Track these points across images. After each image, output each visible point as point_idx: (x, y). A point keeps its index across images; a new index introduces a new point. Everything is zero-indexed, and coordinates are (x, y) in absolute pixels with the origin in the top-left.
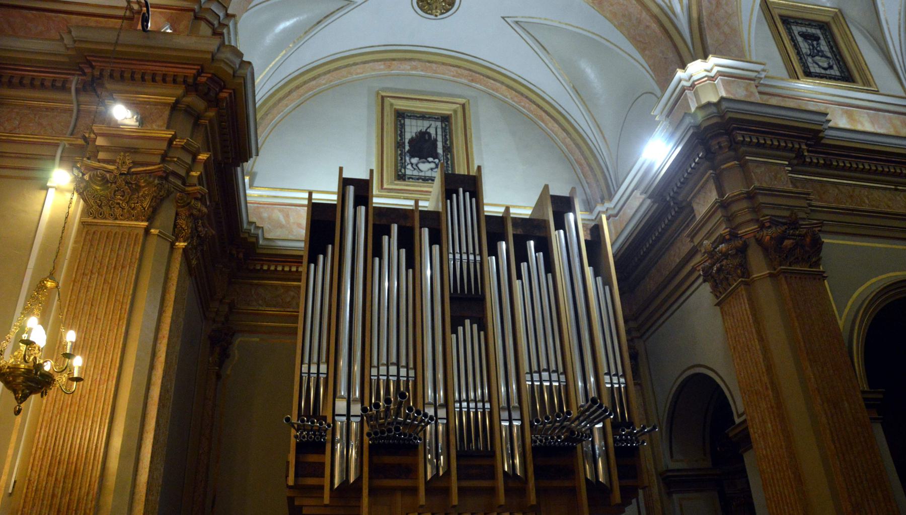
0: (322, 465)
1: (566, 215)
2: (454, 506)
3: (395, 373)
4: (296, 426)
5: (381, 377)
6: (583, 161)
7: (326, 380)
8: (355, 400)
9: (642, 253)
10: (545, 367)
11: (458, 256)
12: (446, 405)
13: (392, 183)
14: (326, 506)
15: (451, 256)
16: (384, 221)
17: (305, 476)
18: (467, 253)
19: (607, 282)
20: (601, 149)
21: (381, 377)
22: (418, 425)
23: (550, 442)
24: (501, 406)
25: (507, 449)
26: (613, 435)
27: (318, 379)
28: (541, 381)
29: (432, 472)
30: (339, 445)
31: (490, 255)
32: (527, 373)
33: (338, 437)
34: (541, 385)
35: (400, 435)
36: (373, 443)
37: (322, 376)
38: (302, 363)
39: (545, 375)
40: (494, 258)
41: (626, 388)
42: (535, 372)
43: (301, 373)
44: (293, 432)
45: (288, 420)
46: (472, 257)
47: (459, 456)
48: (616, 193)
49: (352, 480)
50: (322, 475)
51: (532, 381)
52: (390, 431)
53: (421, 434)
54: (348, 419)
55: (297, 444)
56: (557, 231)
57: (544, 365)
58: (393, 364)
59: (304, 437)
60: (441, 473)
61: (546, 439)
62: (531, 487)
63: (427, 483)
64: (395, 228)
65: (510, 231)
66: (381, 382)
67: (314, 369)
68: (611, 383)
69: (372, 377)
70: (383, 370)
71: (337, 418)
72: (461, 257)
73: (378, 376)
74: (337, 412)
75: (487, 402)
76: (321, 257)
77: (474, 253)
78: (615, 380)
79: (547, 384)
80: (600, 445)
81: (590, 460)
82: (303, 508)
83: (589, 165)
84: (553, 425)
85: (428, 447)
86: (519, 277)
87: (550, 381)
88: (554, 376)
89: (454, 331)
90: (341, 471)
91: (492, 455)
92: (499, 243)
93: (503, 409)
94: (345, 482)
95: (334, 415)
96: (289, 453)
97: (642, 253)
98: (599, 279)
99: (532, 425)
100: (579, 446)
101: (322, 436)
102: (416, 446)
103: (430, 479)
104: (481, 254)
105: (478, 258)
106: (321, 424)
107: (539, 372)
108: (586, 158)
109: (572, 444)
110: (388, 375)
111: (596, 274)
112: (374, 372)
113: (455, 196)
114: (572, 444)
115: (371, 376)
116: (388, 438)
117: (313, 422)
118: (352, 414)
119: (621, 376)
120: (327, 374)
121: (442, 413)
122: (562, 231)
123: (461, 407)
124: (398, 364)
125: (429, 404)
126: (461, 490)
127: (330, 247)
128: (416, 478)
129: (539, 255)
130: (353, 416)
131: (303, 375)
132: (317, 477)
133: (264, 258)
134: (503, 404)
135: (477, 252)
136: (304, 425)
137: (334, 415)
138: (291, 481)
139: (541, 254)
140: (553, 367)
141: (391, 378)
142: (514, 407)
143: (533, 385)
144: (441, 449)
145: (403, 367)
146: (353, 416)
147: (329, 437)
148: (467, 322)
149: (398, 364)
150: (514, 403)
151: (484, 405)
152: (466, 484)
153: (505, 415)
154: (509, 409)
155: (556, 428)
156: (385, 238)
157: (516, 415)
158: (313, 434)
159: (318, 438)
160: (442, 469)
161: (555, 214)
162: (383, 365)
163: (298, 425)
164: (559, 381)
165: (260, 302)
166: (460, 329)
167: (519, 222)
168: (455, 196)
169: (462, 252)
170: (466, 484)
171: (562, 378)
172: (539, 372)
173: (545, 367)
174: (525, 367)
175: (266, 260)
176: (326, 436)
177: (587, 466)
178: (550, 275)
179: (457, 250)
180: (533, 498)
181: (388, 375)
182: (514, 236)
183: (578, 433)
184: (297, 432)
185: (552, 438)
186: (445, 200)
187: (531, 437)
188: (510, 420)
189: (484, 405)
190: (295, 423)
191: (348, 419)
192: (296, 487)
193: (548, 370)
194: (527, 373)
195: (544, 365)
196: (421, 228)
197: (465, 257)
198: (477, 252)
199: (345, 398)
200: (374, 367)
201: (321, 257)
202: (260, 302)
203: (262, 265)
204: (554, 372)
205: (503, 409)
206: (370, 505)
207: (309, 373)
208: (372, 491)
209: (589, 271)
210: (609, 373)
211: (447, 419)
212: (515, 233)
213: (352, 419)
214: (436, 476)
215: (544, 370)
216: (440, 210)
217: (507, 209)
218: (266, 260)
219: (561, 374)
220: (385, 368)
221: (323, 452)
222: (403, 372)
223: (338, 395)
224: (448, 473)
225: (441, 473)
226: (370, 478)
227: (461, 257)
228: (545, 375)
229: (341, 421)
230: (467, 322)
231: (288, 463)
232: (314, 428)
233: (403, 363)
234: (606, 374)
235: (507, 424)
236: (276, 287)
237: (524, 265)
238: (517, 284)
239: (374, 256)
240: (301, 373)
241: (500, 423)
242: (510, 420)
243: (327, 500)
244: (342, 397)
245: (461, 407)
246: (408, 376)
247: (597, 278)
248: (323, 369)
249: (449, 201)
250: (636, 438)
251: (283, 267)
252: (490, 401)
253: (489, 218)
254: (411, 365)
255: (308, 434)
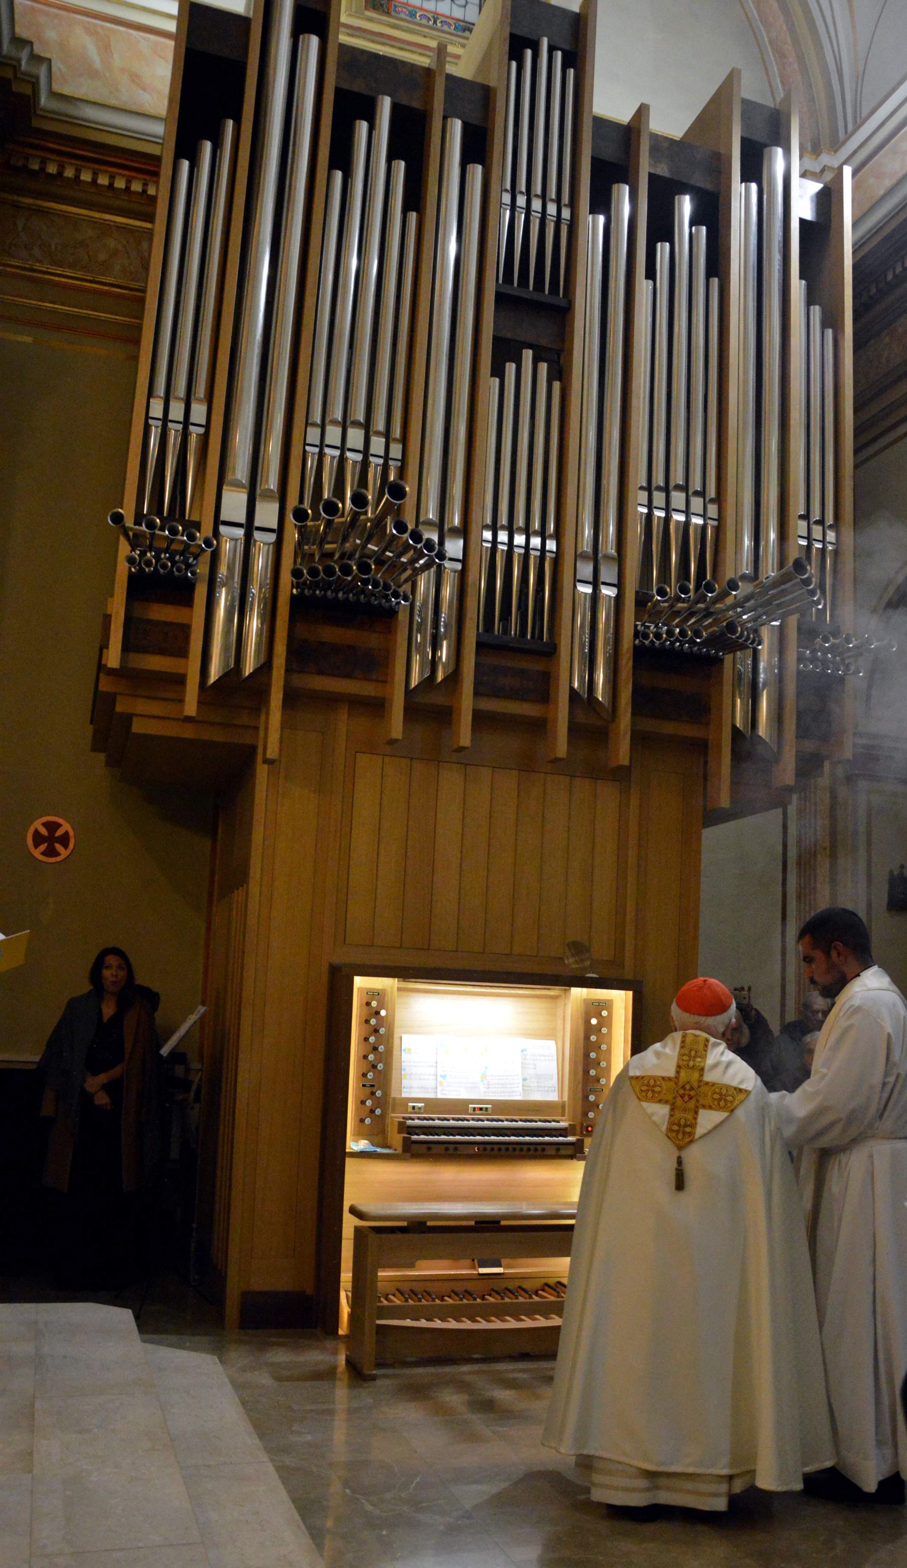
0: (185, 629)
1: (766, 150)
2: (461, 749)
3: (360, 446)
4: (131, 534)
5: (327, 450)
6: (788, 47)
7: (205, 439)
8: (268, 495)
9: (890, 277)
10: (681, 482)
11: (521, 201)
12: (464, 531)
13: (358, 15)
14: (188, 719)
15: (507, 198)
16: (359, 86)
17: (144, 650)
18: (544, 197)
19: (832, 320)
20: (835, 24)
21: (327, 450)
22: (404, 567)
23: (672, 643)
24: (579, 551)
25: (582, 646)
26: (798, 647)
27: (185, 434)
28: (667, 509)
29: (422, 671)
30: (224, 590)
31: (593, 211)
32: (641, 488)
33: (223, 570)
34: (667, 519)
35: (365, 582)
36: (301, 594)
37: (195, 432)
38: (150, 394)
39: (678, 499)
40: (601, 219)
41: (836, 553)
42: (659, 488)
43: (147, 417)
44: (124, 548)
45: (118, 519)
46: (552, 209)
47: (480, 645)
48: (849, 136)
49: (248, 668)
50: (183, 653)
51: (650, 506)
52: (346, 570)
53: (407, 587)
54: (248, 537)
55: (131, 577)
56: (743, 184)
57: (678, 477)
58: (356, 424)
59: (148, 563)
60: (440, 677)
61: (670, 633)
62: (622, 726)
63: (408, 692)
64: (385, 105)
65: (645, 167)
66: (327, 461)
67: (177, 411)
68: (808, 538)
69: (308, 448)
70: (333, 434)
71: (223, 529)
72: (529, 202)
73: (322, 445)
74: (224, 517)
75: (551, 537)
76: (208, 146)
77: (558, 200)
78: (817, 531)
79: (680, 518)
80: (769, 662)
81: (746, 689)
82: (135, 720)
83: (801, 58)
84: (689, 609)
85: (417, 619)
86: (651, 274)
87: (687, 512)
88: (697, 503)
89: (498, 371)
90: (225, 648)
91: (550, 651)
92: (615, 187)
93: (584, 556)
94: (232, 673)
95: (217, 522)
96: (112, 596)
97: (890, 277)
98: (816, 310)
99: (642, 601)
100: (728, 659)
101: (189, 566)
102: (392, 613)
103: (416, 687)
104: (573, 204)
105: (566, 214)
106: (192, 537)
107: (666, 489)
108: (796, 42)
109: (717, 652)
110: (343, 448)
111: (810, 300)
112: (313, 435)
113: (529, 53)
114: (717, 652)
115: (305, 444)
116: (327, 586)
117: (173, 532)
118: (257, 523)
119: (830, 527)
120: (208, 426)
121: (454, 547)
122: (754, 187)
123: (495, 541)
124: (367, 426)
125: (429, 523)
126: (480, 719)
127: (230, 123)
128: (385, 680)
129: (698, 231)
130: (259, 529)
131: (151, 422)
132: (172, 654)
133: (51, 145)
134: (586, 545)
135: (566, 199)
136: (153, 535)
137: (217, 522)
138: (113, 658)
139: (704, 229)
140: (697, 485)
141: (349, 454)
142: (607, 557)
143: (649, 516)
144: (446, 627)
145: (378, 433)
146: (259, 529)
147: (203, 569)
148: (528, 355)
149: (367, 426)
150: (609, 546)
151: (543, 544)
152: (490, 705)
153: (586, 570)
154: (595, 557)
155: (692, 614)
156: (363, 127)
157: (608, 573)
158: (168, 559)
159: (179, 570)
160: (444, 668)
161: (745, 142)
162: (334, 422)
163: (136, 535)
164: (704, 516)
165: (37, 252)
166: (511, 368)
167: (662, 145)
168: (529, 53)
169: (533, 193)
170: (490, 705)
171: (713, 510)
172: (666, 489)
173: (661, 483)
174: (638, 475)
175: (53, 151)
176: (196, 565)
177: (739, 701)
178: (715, 282)
179: (522, 186)
180: (622, 752)
181: (343, 448)
182: (652, 178)
183: (741, 635)
184: (133, 550)
185: (683, 633)
186: (506, 57)
187: (636, 626)
188: (595, 583)
189: (543, 544)
190: (131, 529)
191: (248, 537)
192: (123, 673)
193: (684, 488)
194: (641, 488)
195: (678, 477)
196: (445, 118)
197: (537, 205)
198: (566, 199)
199: (243, 486)
200: (314, 425)
201: (208, 146)
202: (37, 252)
203: (44, 162)
204: (696, 493)
205: (584, 556)
206: (284, 725)
207: (165, 419)
208: (291, 698)
209: (797, 286)
210: (806, 517)
211: (464, 561)
212: (652, 171)
213: (257, 535)
214: (429, 681)
215: (678, 488)
216: (493, 81)
217: (642, 112)
218: (53, 151)
219: (712, 501)
220: (339, 430)
221: (187, 601)
222: (377, 445)
223: (229, 477)
224: (454, 677)
225: (440, 677)
226: (288, 671)
227: (529, 202)
228: (678, 499)
229: (232, 536)
230: (528, 355)
231: (107, 619)
232: (174, 547)
233: (380, 424)
234: (801, 517)
235: (588, 590)
236: (74, 222)
237: (662, 249)
238: (643, 287)
239: (332, 166)
240: (147, 417)
241: (575, 587)
242: (595, 583)
243: (191, 707)
244: (237, 485)
245: (495, 541)
246: (386, 457)
247: (812, 307)
248: (199, 412)
249: (514, 64)
250: (843, 660)
251: (95, 174)
252: (558, 536)
253: (599, 122)
254: (397, 432)
255: (157, 557)
